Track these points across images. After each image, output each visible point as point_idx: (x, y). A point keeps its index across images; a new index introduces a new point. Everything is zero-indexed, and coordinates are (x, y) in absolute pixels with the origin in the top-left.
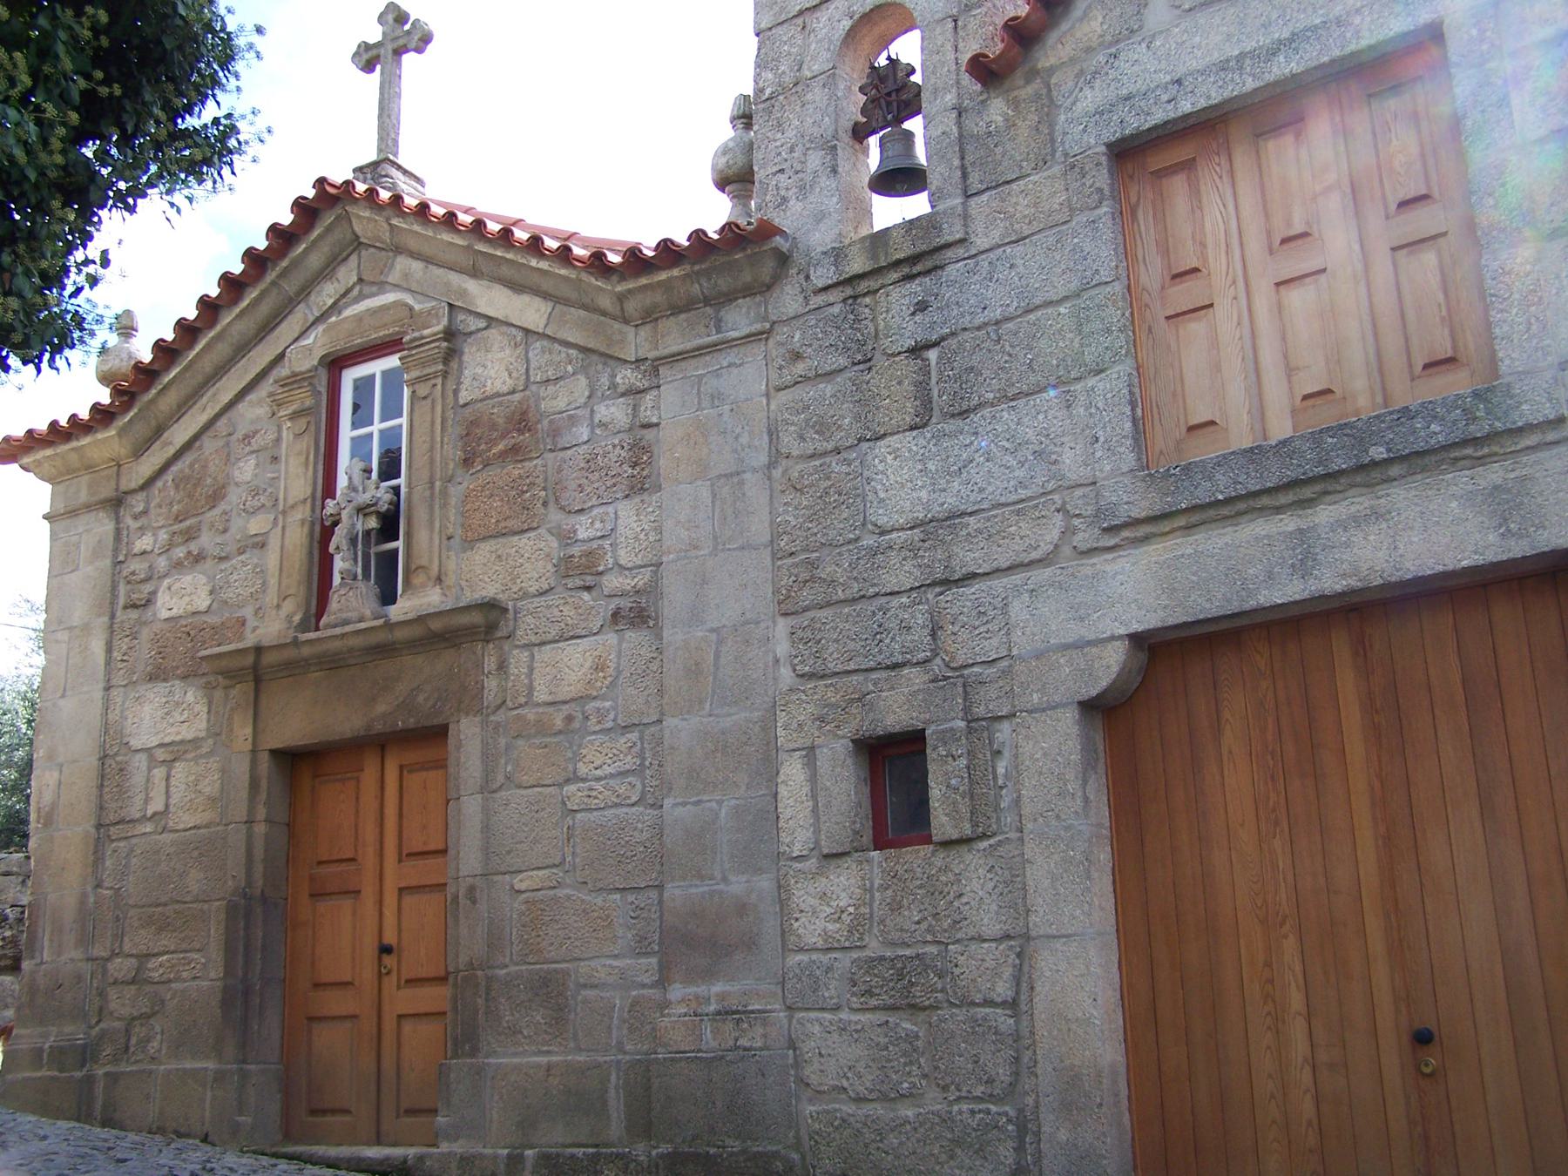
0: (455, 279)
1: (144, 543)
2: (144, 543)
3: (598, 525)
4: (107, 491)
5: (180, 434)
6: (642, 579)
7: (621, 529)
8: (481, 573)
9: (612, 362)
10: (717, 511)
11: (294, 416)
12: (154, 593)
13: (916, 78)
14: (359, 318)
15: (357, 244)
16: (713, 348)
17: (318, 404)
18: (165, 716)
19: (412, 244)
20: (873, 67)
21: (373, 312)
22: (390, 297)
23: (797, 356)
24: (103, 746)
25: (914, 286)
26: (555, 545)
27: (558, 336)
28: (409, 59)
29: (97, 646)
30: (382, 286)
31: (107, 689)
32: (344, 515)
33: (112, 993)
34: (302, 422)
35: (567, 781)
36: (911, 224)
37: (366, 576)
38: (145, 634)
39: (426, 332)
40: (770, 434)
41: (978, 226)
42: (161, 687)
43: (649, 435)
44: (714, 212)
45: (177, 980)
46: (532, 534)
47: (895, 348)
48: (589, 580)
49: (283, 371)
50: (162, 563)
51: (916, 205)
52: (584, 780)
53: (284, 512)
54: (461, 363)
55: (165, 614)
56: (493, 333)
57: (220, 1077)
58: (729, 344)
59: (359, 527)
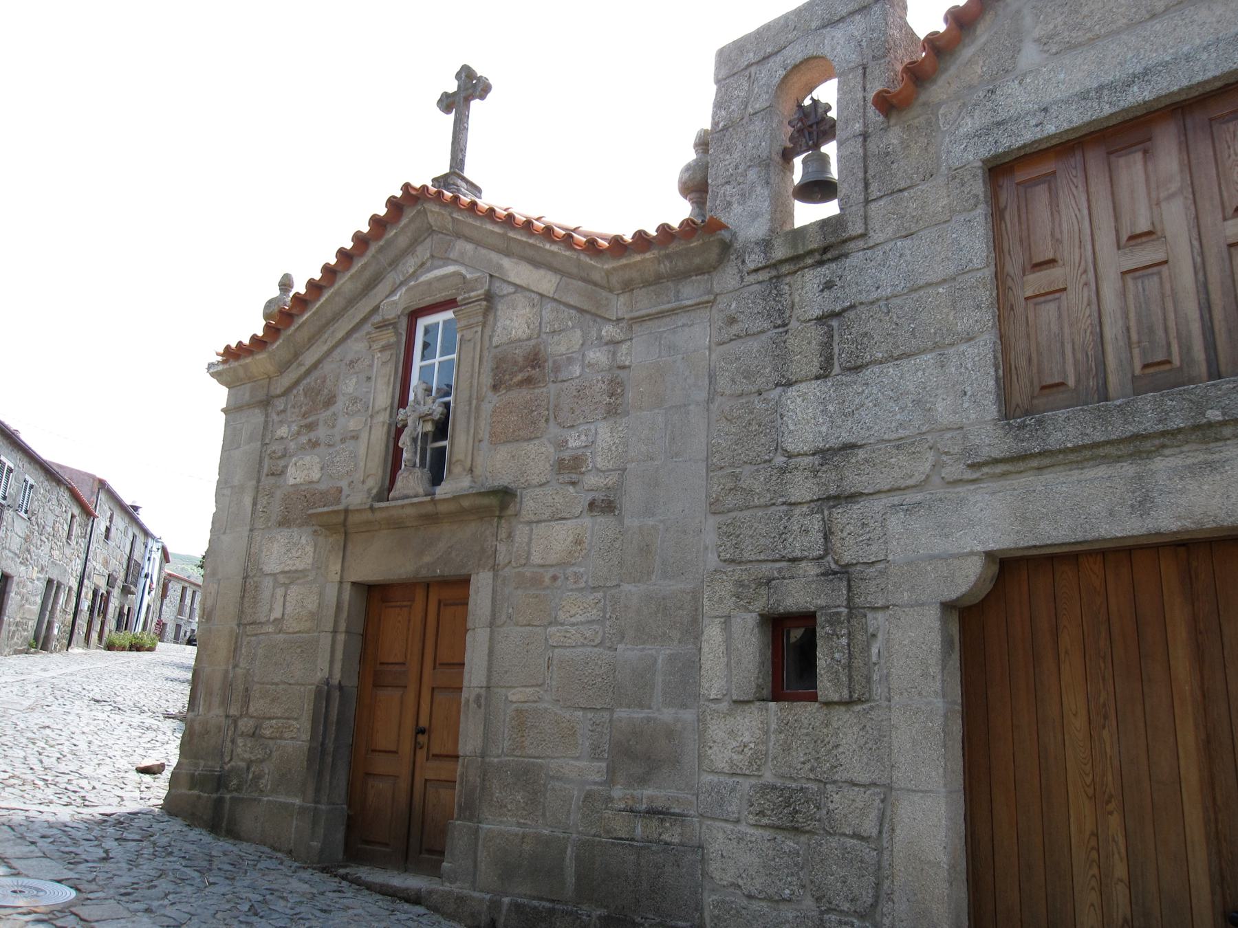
0: (494, 256)
1: (283, 431)
2: (283, 431)
3: (583, 437)
4: (261, 395)
5: (309, 358)
6: (611, 480)
7: (599, 442)
8: (498, 465)
9: (598, 320)
10: (669, 432)
11: (383, 349)
12: (286, 467)
13: (833, 114)
14: (429, 283)
15: (430, 231)
16: (673, 311)
17: (398, 342)
18: (288, 551)
19: (467, 231)
20: (800, 107)
21: (440, 279)
22: (451, 269)
23: (732, 320)
24: (246, 570)
25: (823, 270)
26: (552, 450)
27: (563, 300)
28: (475, 104)
29: (248, 501)
30: (447, 261)
31: (251, 530)
32: (410, 422)
33: (240, 742)
34: (388, 353)
35: (550, 624)
36: (824, 224)
37: (423, 464)
38: (279, 494)
39: (472, 294)
40: (710, 377)
41: (875, 224)
42: (286, 532)
43: (623, 374)
44: (679, 211)
45: (281, 738)
46: (536, 442)
47: (808, 316)
48: (574, 477)
49: (376, 319)
50: (292, 446)
51: (830, 209)
52: (562, 624)
53: (372, 417)
54: (495, 316)
55: (291, 481)
56: (519, 297)
57: (302, 810)
58: (685, 309)
59: (420, 429)
